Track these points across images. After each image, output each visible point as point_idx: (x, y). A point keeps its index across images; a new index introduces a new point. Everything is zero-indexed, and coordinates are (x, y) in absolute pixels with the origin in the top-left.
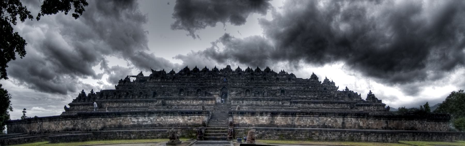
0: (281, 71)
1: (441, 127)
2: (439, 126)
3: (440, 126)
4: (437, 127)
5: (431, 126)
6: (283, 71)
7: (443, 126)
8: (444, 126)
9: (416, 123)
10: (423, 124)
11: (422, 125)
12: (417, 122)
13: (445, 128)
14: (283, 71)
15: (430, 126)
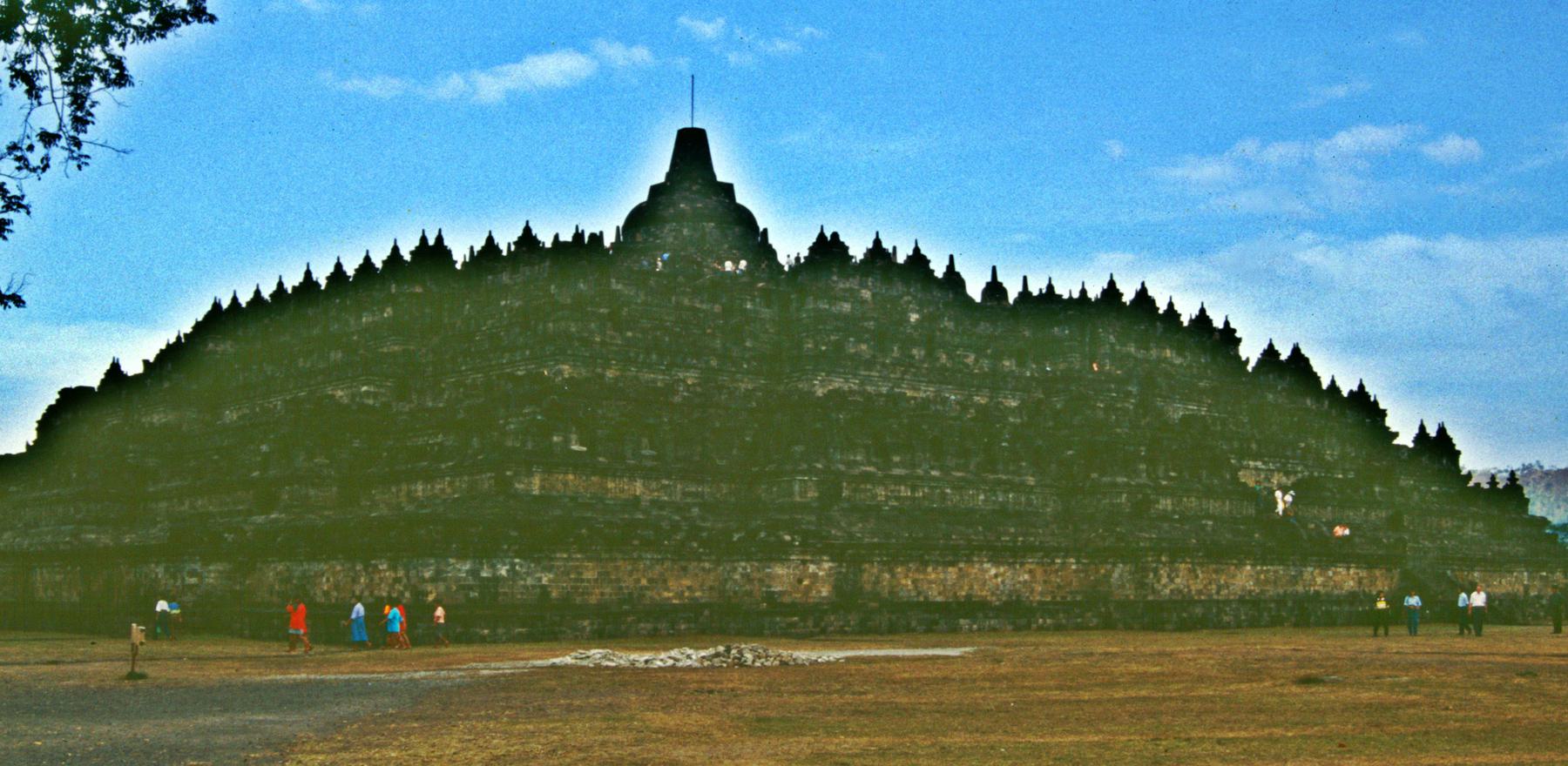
0: (424, 239)
1: (379, 585)
2: (372, 580)
3: (376, 577)
4: (359, 583)
5: (331, 579)
6: (431, 242)
7: (390, 581)
8: (397, 580)
9: (157, 574)
10: (179, 576)
11: (176, 581)
12: (160, 570)
13: (399, 587)
14: (431, 242)
15: (328, 580)
